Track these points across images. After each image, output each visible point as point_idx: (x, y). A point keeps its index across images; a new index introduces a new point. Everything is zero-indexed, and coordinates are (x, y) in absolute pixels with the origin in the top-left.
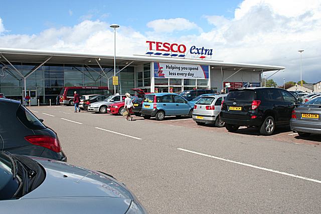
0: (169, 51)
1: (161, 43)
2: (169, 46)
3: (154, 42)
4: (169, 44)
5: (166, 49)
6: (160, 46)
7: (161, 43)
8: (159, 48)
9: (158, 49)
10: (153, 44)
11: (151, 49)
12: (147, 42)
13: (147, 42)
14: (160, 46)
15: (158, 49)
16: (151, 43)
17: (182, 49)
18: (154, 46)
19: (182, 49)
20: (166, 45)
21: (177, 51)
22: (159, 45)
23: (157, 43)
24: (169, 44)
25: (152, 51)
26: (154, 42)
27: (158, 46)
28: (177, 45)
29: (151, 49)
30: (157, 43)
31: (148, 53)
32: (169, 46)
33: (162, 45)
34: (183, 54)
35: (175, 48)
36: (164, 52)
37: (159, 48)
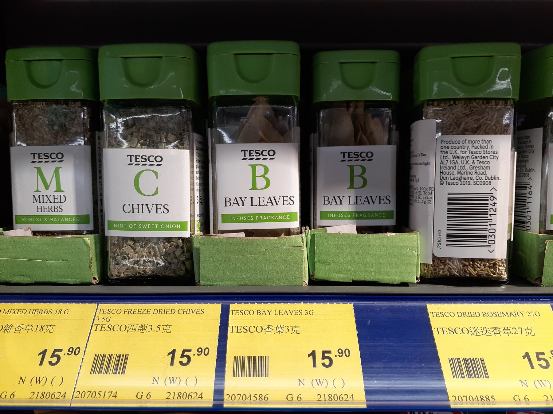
0: (146, 161)
1: (139, 156)
3: (133, 156)
4: (146, 156)
5: (145, 160)
6: (138, 159)
7: (139, 156)
8: (138, 160)
9: (136, 161)
10: (132, 157)
11: (131, 161)
12: (128, 156)
13: (128, 156)
14: (138, 159)
16: (131, 156)
17: (159, 159)
18: (133, 159)
19: (159, 159)
21: (153, 162)
23: (136, 156)
24: (146, 156)
26: (133, 156)
27: (136, 159)
28: (153, 156)
29: (131, 161)
30: (136, 156)
31: (129, 164)
33: (140, 158)
35: (152, 159)
37: (138, 160)
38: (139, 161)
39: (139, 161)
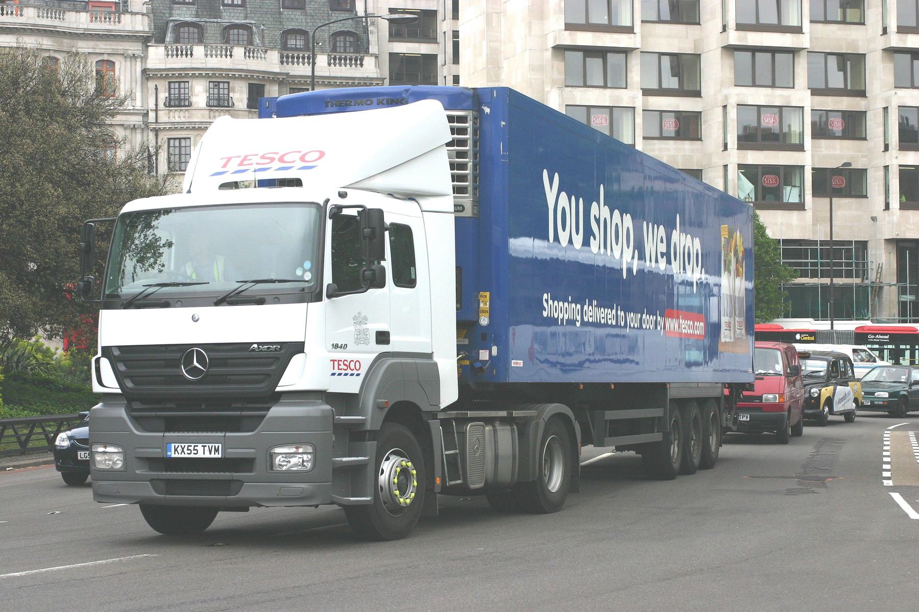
2: (348, 364)
3: (336, 361)
4: (347, 361)
5: (345, 368)
6: (340, 365)
7: (341, 361)
8: (340, 367)
9: (339, 369)
11: (334, 369)
13: (331, 360)
14: (340, 365)
15: (339, 369)
16: (334, 361)
18: (336, 363)
20: (345, 362)
22: (340, 363)
25: (334, 372)
27: (339, 365)
29: (334, 369)
30: (339, 361)
32: (348, 364)
34: (358, 372)
35: (352, 366)
36: (343, 372)
37: (340, 367)
38: (341, 369)
39: (341, 369)
